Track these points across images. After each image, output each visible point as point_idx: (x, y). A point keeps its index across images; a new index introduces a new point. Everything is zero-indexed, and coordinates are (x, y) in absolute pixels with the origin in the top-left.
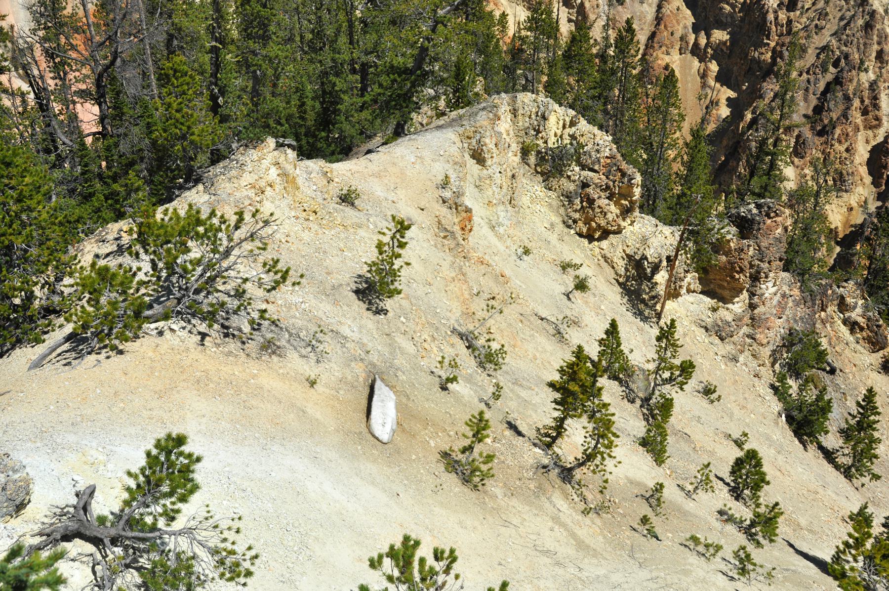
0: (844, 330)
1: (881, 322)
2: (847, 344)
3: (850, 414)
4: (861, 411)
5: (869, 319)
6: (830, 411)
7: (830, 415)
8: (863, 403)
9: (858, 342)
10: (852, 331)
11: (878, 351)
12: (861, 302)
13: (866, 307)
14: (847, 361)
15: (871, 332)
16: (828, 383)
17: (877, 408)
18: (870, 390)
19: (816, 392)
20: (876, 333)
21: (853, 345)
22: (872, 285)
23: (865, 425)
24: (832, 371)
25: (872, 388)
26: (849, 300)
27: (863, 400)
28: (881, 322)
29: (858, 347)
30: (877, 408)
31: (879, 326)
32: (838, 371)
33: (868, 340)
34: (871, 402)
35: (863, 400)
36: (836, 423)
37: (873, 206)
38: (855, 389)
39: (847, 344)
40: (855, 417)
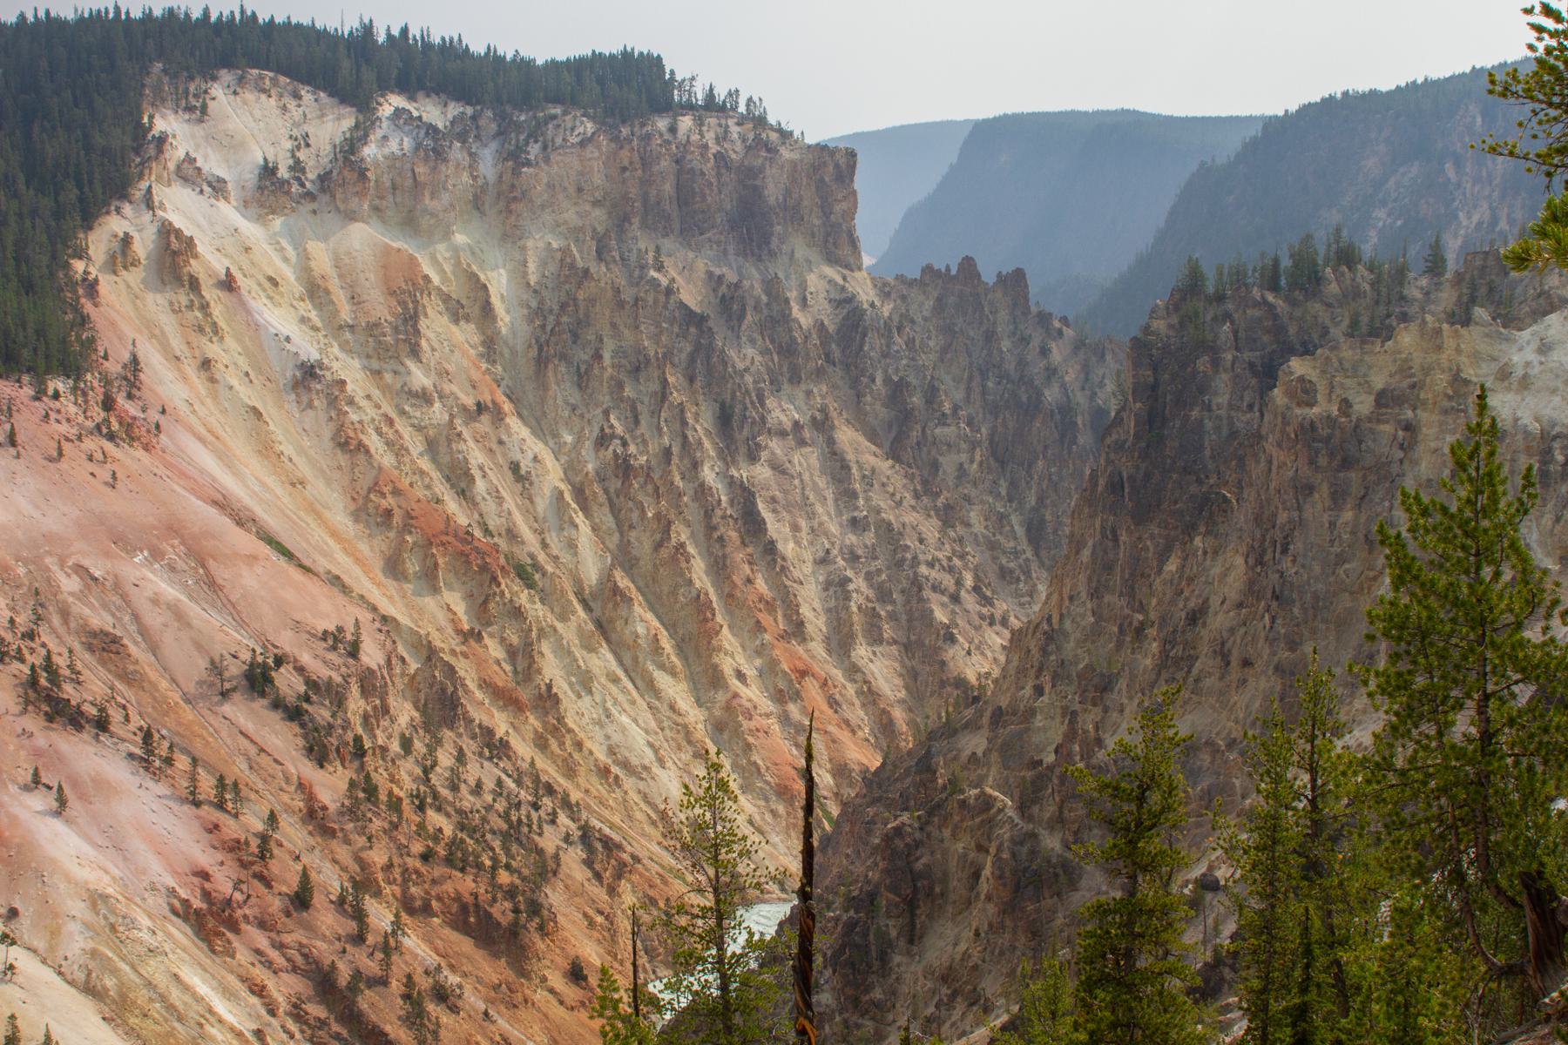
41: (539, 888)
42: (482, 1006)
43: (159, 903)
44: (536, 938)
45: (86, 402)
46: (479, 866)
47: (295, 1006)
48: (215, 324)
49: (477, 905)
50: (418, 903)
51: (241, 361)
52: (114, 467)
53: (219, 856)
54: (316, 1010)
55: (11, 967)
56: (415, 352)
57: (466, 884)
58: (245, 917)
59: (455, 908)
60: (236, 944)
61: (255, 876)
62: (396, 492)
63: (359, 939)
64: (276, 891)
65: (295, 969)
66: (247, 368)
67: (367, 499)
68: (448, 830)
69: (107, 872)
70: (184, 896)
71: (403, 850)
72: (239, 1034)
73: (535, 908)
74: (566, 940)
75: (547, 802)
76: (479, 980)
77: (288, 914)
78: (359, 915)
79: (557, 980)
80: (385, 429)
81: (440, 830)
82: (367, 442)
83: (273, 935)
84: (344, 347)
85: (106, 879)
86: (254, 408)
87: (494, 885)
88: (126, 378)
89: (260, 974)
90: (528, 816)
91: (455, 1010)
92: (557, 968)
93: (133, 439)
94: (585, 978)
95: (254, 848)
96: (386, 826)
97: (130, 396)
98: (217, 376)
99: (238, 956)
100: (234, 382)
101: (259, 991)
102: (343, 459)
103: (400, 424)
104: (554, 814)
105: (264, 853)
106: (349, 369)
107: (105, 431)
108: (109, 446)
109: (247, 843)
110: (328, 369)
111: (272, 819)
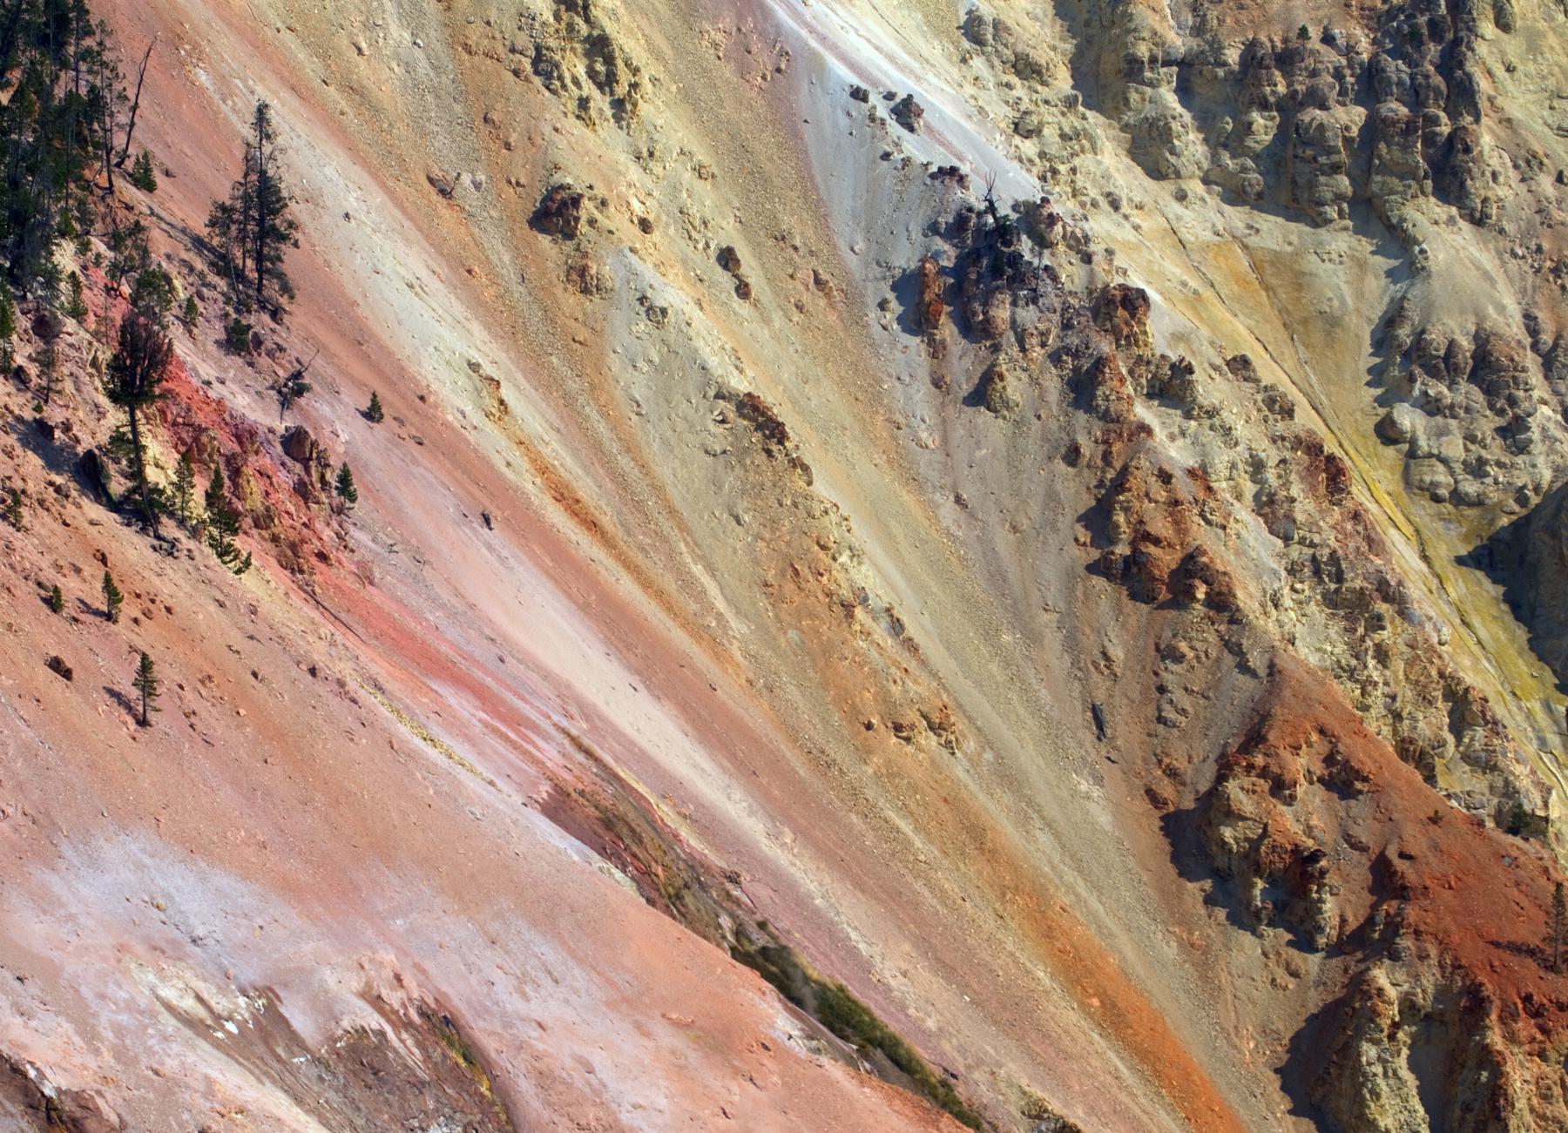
45: (47, 361)
48: (599, 46)
51: (705, 200)
52: (149, 638)
56: (1449, 173)
62: (1342, 780)
66: (727, 233)
67: (1214, 805)
80: (1304, 508)
82: (1219, 553)
84: (1150, 148)
86: (751, 407)
88: (223, 265)
93: (227, 519)
97: (238, 341)
98: (605, 268)
100: (674, 295)
102: (1119, 627)
103: (1374, 481)
106: (1161, 237)
107: (118, 486)
108: (130, 547)
110: (1081, 248)
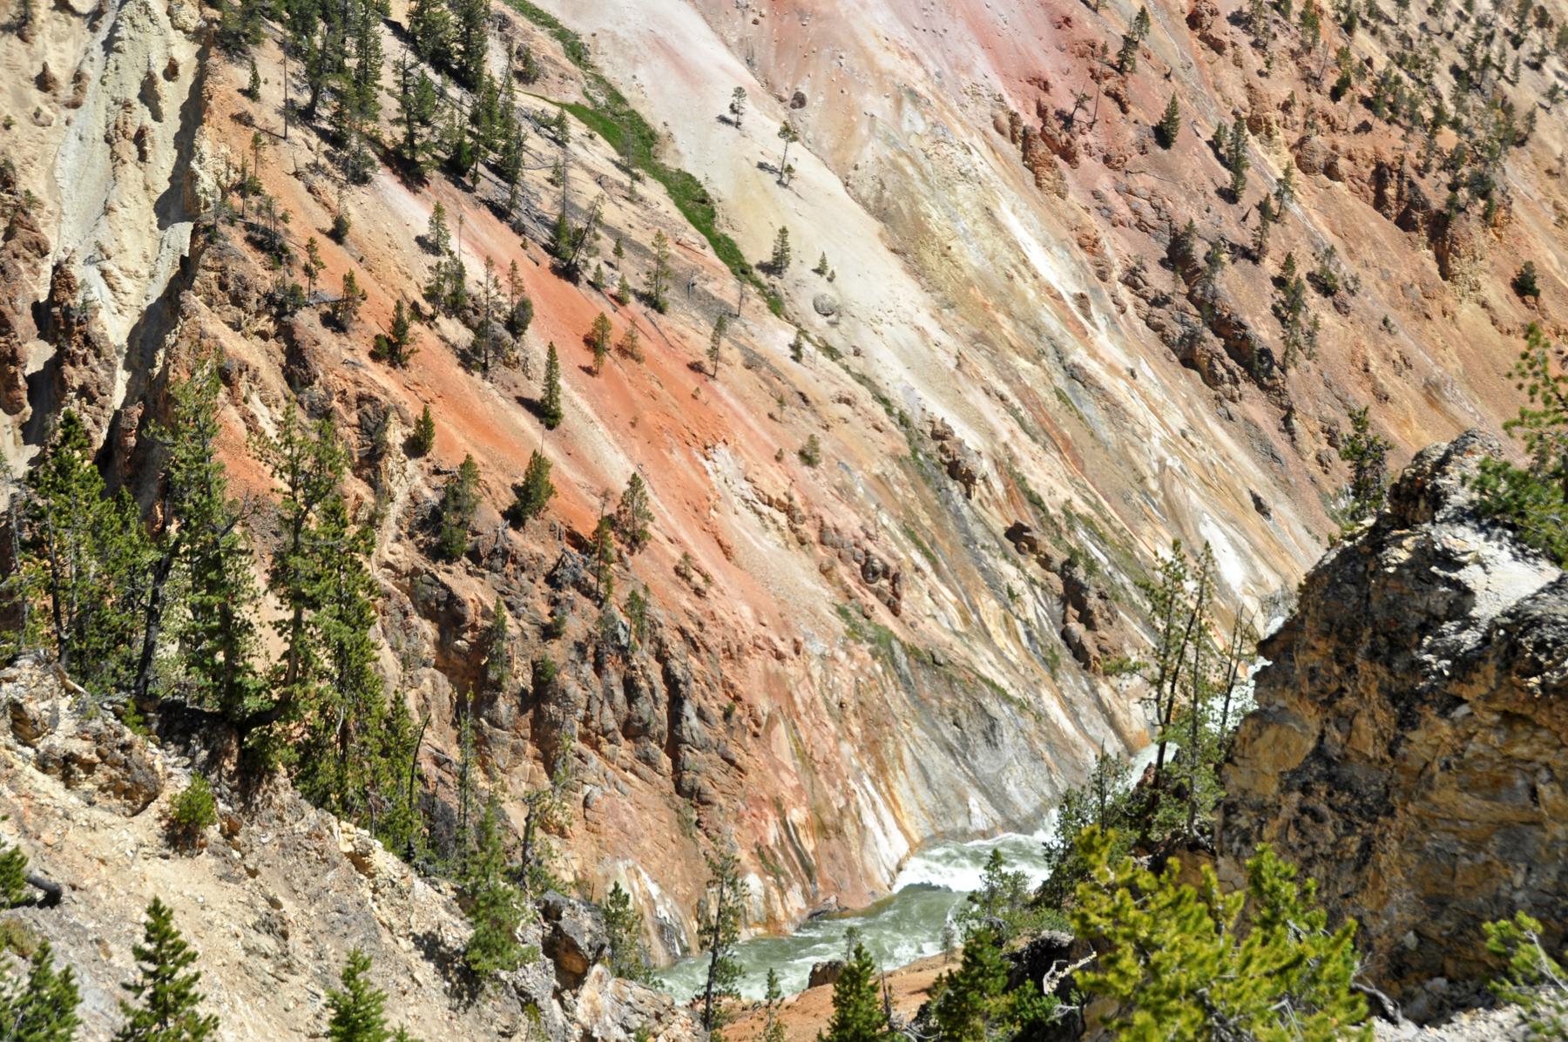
0: (49, 785)
1: (128, 735)
2: (67, 816)
3: (126, 987)
4: (152, 967)
5: (98, 738)
6: (75, 1001)
7: (78, 1011)
8: (149, 947)
9: (91, 803)
10: (68, 780)
11: (144, 807)
12: (64, 703)
13: (82, 711)
14: (79, 857)
15: (114, 765)
16: (52, 930)
17: (183, 946)
18: (155, 909)
19: (25, 966)
20: (126, 766)
21: (82, 814)
22: (81, 653)
23: (171, 998)
24: (53, 898)
25: (156, 901)
26: (34, 708)
27: (148, 939)
28: (128, 735)
29: (97, 814)
30: (183, 946)
31: (125, 747)
32: (66, 892)
33: (114, 788)
34: (167, 935)
35: (148, 939)
36: (104, 1024)
37: (20, 459)
38: (123, 918)
39: (67, 816)
40: (143, 988)
41: (1494, 156)
42: (1381, 311)
43: (982, 112)
44: (1475, 225)
46: (1414, 117)
47: (1133, 272)
49: (1401, 175)
50: (1319, 160)
53: (1066, 62)
54: (1160, 280)
55: (789, 169)
57: (1388, 141)
58: (1086, 146)
59: (1367, 174)
60: (1070, 180)
61: (1108, 94)
63: (1230, 196)
64: (1132, 117)
65: (1142, 226)
68: (1381, 62)
69: (920, 64)
70: (1014, 108)
71: (1311, 79)
72: (1058, 297)
73: (1482, 187)
74: (1518, 237)
75: (1535, 38)
76: (1385, 276)
77: (1143, 150)
78: (1234, 163)
79: (1497, 291)
81: (1369, 62)
83: (1120, 175)
85: (920, 72)
87: (1430, 146)
89: (1095, 223)
90: (1503, 55)
91: (1341, 308)
92: (1501, 273)
94: (1536, 294)
95: (1112, 56)
96: (1296, 46)
99: (1071, 196)
101: (1090, 245)
104: (1543, 54)
105: (1121, 67)
109: (1105, 49)
111: (1143, 16)
